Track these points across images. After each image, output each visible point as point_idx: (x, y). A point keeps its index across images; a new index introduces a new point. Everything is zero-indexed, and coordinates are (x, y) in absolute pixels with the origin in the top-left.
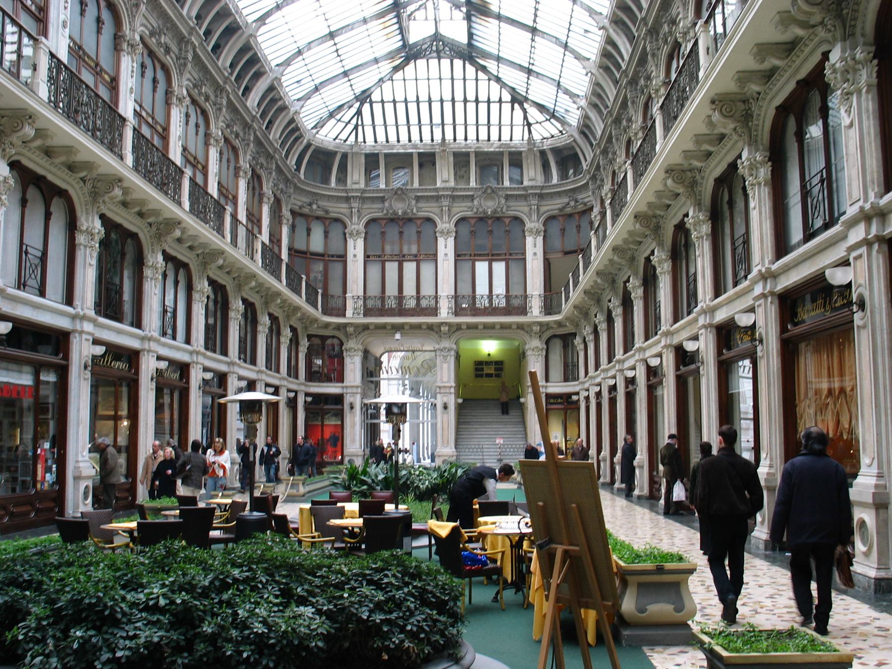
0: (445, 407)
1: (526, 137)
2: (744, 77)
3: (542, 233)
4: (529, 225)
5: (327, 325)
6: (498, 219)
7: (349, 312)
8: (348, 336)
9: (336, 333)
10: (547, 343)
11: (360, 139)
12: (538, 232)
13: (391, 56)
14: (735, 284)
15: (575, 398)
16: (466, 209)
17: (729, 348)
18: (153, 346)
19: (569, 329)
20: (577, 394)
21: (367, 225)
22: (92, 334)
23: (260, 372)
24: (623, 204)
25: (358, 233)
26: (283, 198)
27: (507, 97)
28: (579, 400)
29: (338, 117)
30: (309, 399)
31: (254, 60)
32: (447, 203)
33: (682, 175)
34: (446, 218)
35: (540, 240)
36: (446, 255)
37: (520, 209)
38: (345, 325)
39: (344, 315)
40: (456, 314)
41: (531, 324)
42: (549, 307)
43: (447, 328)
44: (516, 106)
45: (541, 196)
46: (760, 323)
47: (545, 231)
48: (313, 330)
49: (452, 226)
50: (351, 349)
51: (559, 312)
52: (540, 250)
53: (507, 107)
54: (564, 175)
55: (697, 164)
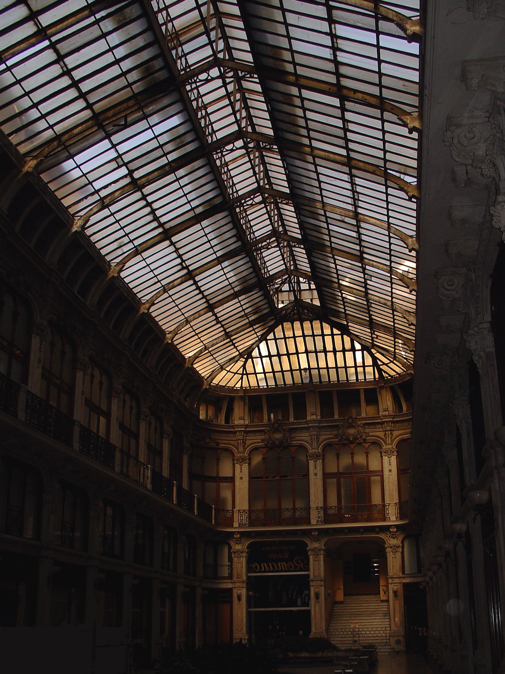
1: (377, 376)
3: (395, 453)
15: (421, 587)
16: (332, 436)
29: (228, 369)
32: (315, 433)
34: (315, 444)
43: (316, 533)
44: (365, 352)
50: (238, 551)
53: (359, 354)
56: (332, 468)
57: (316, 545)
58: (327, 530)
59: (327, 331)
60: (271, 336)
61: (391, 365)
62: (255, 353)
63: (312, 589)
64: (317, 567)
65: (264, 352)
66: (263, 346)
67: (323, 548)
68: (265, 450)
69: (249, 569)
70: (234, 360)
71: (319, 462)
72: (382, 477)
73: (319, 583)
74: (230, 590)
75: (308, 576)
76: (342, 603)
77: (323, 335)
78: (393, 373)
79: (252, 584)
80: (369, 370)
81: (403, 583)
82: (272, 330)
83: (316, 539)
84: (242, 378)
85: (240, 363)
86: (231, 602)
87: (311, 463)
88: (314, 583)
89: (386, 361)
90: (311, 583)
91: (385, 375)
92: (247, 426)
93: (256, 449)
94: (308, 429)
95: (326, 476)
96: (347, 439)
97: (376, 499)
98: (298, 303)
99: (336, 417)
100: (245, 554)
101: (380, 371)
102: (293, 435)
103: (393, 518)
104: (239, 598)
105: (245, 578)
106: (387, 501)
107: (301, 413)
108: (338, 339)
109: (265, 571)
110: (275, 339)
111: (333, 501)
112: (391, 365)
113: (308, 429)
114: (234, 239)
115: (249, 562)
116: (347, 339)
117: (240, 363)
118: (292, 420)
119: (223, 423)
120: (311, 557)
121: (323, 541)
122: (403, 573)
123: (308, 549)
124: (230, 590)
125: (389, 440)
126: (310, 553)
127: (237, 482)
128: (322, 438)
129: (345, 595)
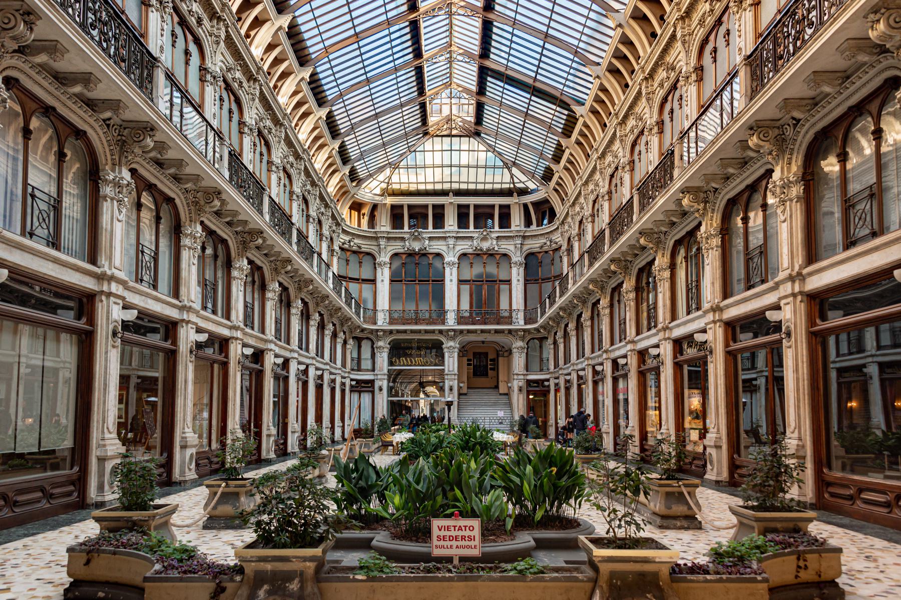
0: (451, 389)
5: (363, 330)
6: (492, 255)
7: (380, 323)
8: (378, 338)
9: (370, 336)
14: (688, 313)
15: (546, 383)
17: (682, 354)
18: (272, 346)
20: (548, 380)
22: (242, 340)
23: (326, 364)
24: (602, 253)
26: (334, 236)
28: (549, 386)
35: (522, 270)
36: (451, 280)
37: (508, 247)
38: (377, 330)
39: (375, 323)
40: (459, 324)
41: (517, 330)
44: (506, 170)
45: (524, 237)
47: (526, 264)
48: (358, 333)
49: (456, 260)
50: (380, 347)
51: (536, 322)
54: (540, 224)
56: (467, 276)
57: (451, 343)
58: (461, 331)
63: (446, 381)
64: (451, 362)
67: (458, 346)
68: (404, 256)
69: (391, 363)
70: (381, 169)
71: (455, 270)
72: (510, 285)
73: (453, 377)
74: (372, 382)
76: (465, 394)
79: (394, 377)
81: (528, 380)
83: (453, 338)
85: (388, 171)
86: (373, 392)
87: (447, 271)
88: (449, 377)
90: (446, 377)
92: (389, 233)
94: (445, 238)
95: (461, 282)
97: (504, 305)
99: (472, 228)
100: (386, 350)
102: (432, 243)
103: (522, 322)
104: (381, 389)
105: (386, 371)
106: (514, 307)
109: (404, 365)
111: (465, 306)
113: (445, 238)
115: (390, 358)
118: (430, 228)
120: (446, 355)
121: (459, 339)
123: (444, 346)
124: (372, 382)
126: (445, 350)
128: (458, 248)
129: (468, 388)
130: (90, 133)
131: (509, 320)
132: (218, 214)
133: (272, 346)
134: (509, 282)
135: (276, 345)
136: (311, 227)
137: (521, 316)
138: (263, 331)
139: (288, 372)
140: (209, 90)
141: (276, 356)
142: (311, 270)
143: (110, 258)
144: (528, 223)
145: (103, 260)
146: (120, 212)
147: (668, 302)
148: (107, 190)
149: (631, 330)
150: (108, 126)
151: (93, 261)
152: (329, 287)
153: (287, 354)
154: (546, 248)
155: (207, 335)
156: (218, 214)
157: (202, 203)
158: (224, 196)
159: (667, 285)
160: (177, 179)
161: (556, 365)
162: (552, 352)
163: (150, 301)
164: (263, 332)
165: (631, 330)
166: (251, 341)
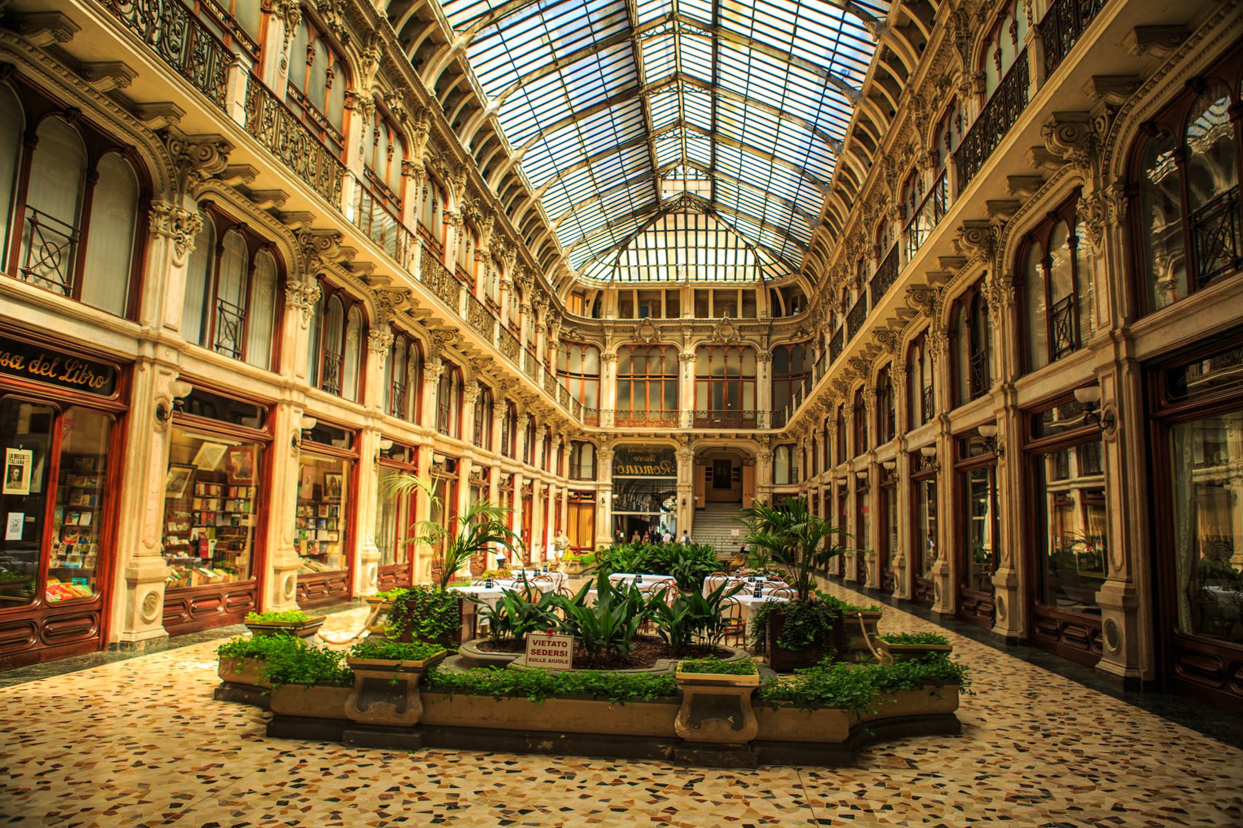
1: (758, 276)
2: (932, 277)
4: (760, 352)
5: (583, 434)
6: (734, 347)
9: (592, 439)
10: (774, 451)
11: (617, 277)
12: (767, 359)
13: (645, 210)
19: (792, 440)
21: (619, 350)
24: (841, 350)
25: (611, 357)
27: (741, 244)
30: (572, 494)
31: (537, 219)
33: (886, 336)
35: (769, 364)
37: (751, 338)
39: (598, 426)
40: (695, 427)
42: (777, 422)
46: (939, 453)
48: (577, 437)
51: (783, 426)
52: (768, 374)
55: (897, 328)
58: (697, 436)
59: (712, 226)
60: (652, 228)
61: (775, 267)
62: (632, 245)
64: (685, 473)
65: (642, 245)
66: (641, 238)
70: (607, 251)
72: (755, 382)
75: (675, 481)
76: (703, 509)
77: (706, 230)
78: (774, 275)
79: (617, 486)
80: (750, 270)
82: (653, 221)
84: (613, 271)
85: (614, 254)
89: (769, 261)
91: (766, 276)
92: (615, 322)
93: (624, 346)
95: (698, 378)
96: (722, 341)
97: (748, 406)
98: (686, 197)
101: (761, 270)
103: (768, 426)
106: (760, 408)
107: (674, 310)
108: (722, 236)
110: (655, 231)
111: (703, 407)
112: (775, 267)
114: (638, 126)
116: (732, 237)
117: (614, 254)
118: (664, 317)
119: (590, 317)
120: (679, 464)
122: (774, 482)
125: (765, 345)
126: (678, 457)
127: (604, 381)
130: (281, 245)
131: (753, 424)
132: (409, 313)
133: (469, 453)
134: (753, 378)
135: (474, 452)
136: (524, 318)
137: (767, 419)
138: (459, 435)
139: (489, 481)
140: (411, 184)
141: (474, 464)
142: (516, 368)
143: (292, 366)
144: (776, 312)
145: (285, 368)
146: (305, 319)
147: (904, 410)
148: (292, 299)
149: (872, 439)
150: (297, 235)
151: (276, 368)
152: (538, 386)
153: (489, 462)
154: (796, 340)
155: (391, 443)
156: (409, 313)
157: (392, 303)
158: (414, 296)
159: (903, 390)
160: (365, 280)
161: (805, 478)
162: (801, 461)
163: (333, 408)
164: (460, 438)
165: (872, 439)
166: (446, 449)
